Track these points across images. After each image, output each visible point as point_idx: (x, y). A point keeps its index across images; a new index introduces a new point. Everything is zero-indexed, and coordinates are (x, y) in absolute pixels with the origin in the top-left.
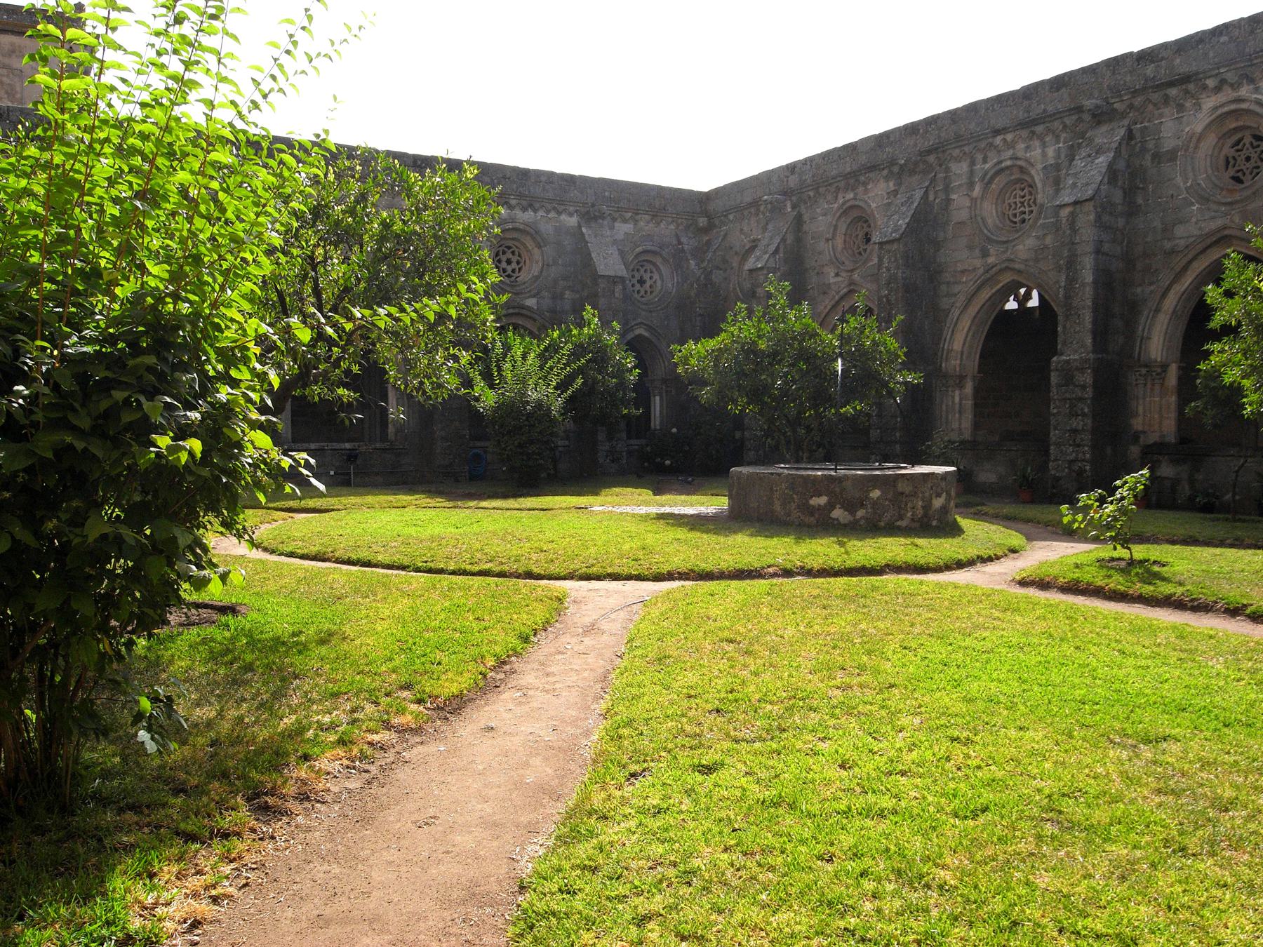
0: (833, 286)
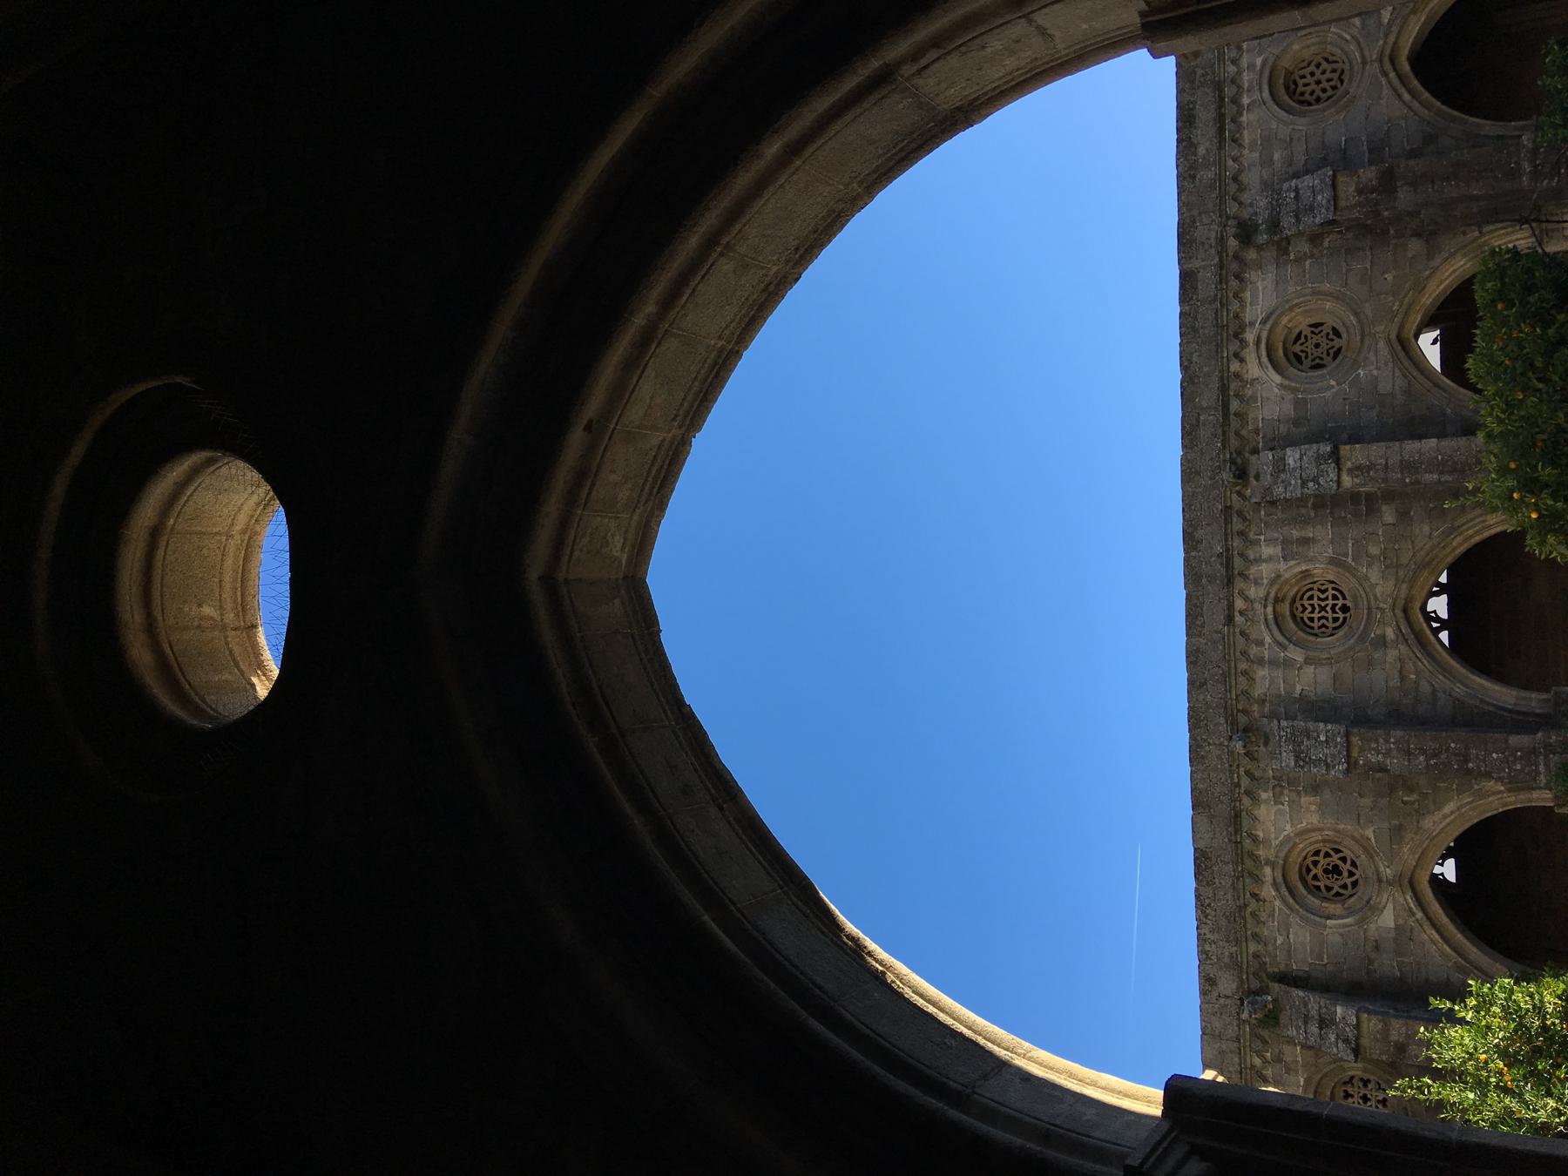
0: (1401, 921)
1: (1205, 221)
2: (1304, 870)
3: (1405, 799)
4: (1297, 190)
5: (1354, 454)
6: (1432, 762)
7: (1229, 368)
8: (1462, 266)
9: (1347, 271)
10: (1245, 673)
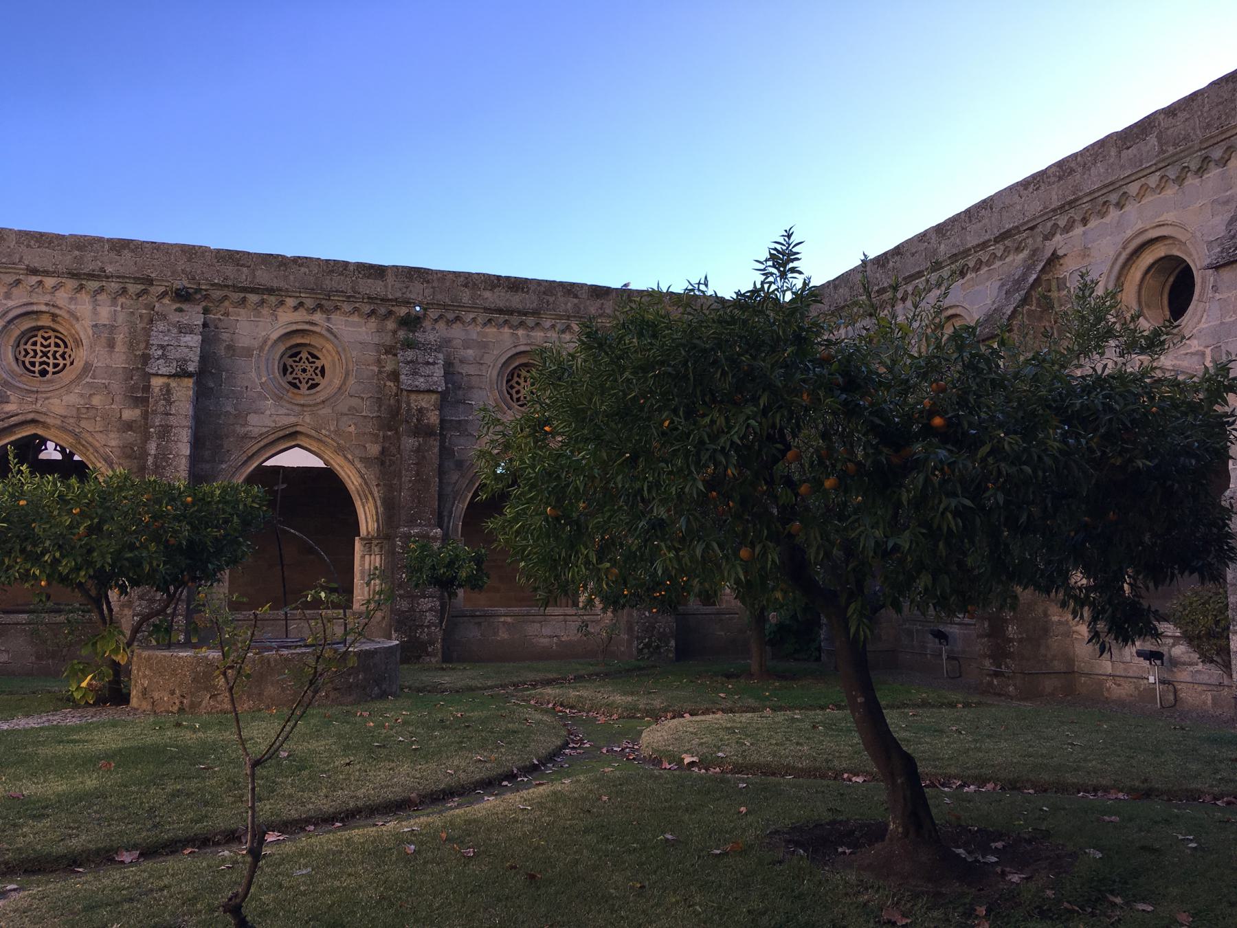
1: (426, 291)
4: (434, 363)
5: (184, 392)
7: (290, 297)
8: (353, 483)
9: (363, 398)
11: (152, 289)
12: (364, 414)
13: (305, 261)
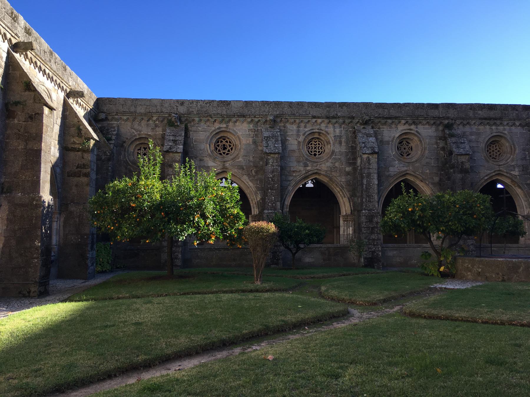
1: (455, 113)
2: (224, 138)
3: (253, 171)
4: (464, 143)
5: (374, 159)
6: (270, 179)
7: (403, 119)
10: (295, 121)
11: (354, 121)
12: (432, 165)
13: (408, 104)
